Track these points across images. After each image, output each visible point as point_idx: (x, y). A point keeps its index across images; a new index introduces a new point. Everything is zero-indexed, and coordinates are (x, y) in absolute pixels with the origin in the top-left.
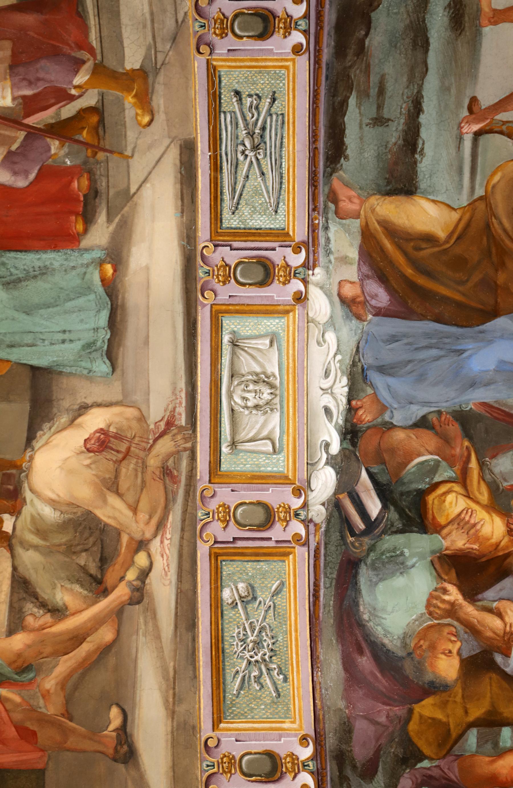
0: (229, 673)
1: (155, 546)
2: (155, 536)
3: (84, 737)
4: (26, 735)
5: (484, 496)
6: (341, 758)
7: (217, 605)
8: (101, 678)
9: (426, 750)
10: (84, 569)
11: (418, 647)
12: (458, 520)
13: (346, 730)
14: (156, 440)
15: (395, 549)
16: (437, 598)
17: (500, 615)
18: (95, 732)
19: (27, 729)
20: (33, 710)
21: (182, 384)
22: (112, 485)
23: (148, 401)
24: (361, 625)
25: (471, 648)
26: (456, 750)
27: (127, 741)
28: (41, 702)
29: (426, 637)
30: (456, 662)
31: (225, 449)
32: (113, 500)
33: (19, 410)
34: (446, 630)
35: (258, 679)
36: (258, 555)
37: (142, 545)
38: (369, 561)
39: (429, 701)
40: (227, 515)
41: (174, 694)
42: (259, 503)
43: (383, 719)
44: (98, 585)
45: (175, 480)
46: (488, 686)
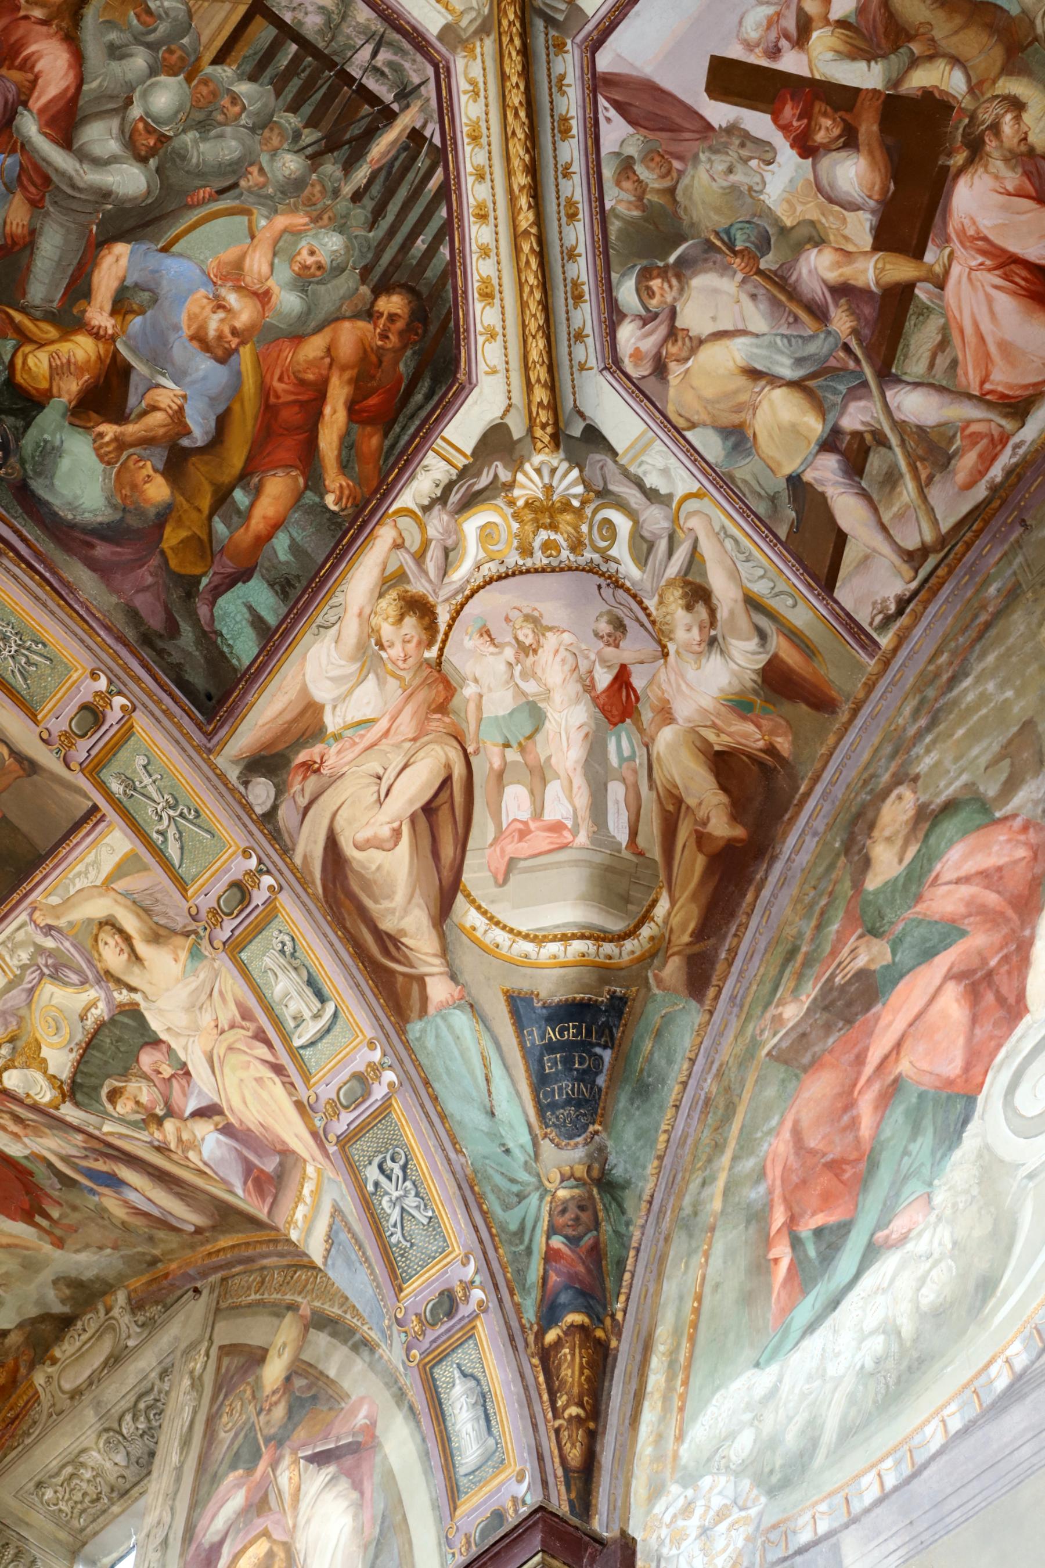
5: (52, 332)
6: (147, 639)
9: (197, 571)
11: (124, 498)
12: (55, 371)
13: (133, 615)
15: (38, 445)
16: (101, 447)
17: (155, 408)
24: (73, 526)
25: (159, 456)
26: (217, 548)
29: (123, 485)
30: (159, 480)
34: (131, 463)
35: (29, 662)
38: (30, 473)
39: (168, 530)
43: (150, 580)
46: (198, 471)
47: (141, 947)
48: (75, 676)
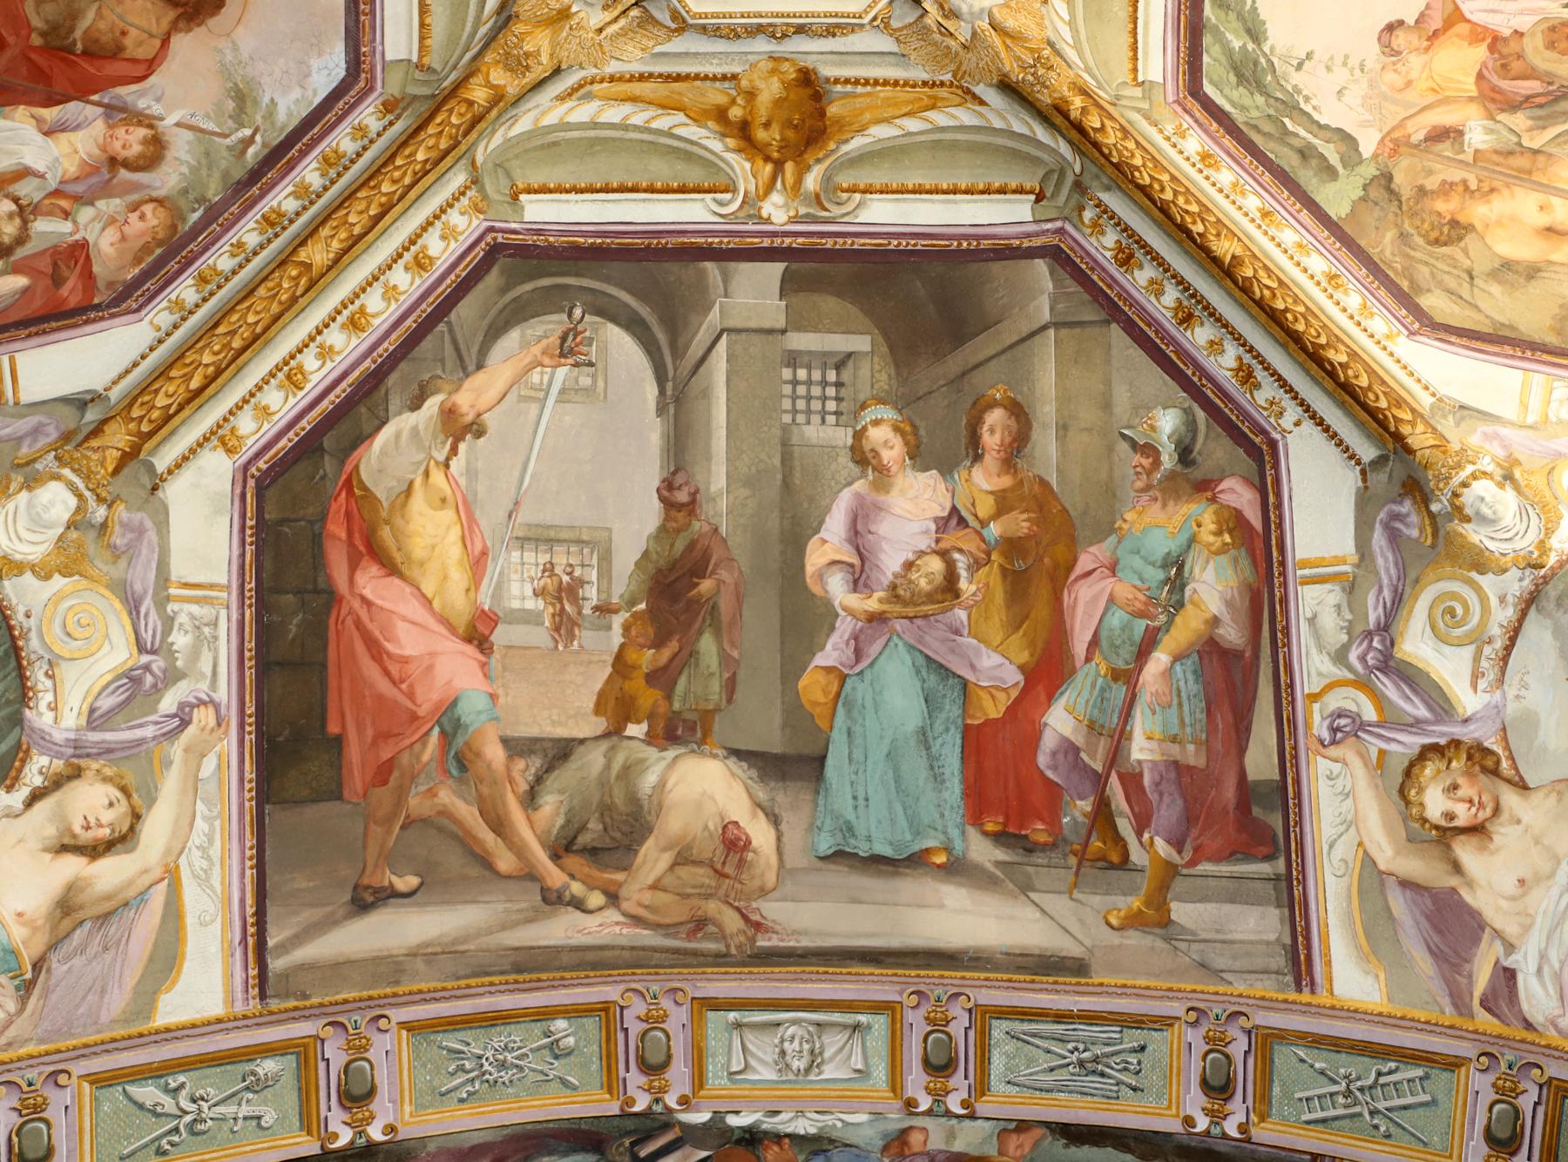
0: (467, 1035)
1: (613, 915)
2: (624, 914)
3: (382, 846)
4: (383, 773)
7: (545, 1014)
8: (453, 860)
10: (583, 828)
14: (738, 909)
18: (391, 860)
19: (390, 773)
20: (413, 778)
21: (805, 943)
22: (684, 858)
23: (785, 900)
27: (379, 900)
28: (422, 788)
31: (732, 1016)
32: (666, 859)
33: (773, 740)
36: (609, 1059)
37: (613, 898)
40: (654, 1020)
41: (436, 954)
42: (669, 1057)
44: (563, 847)
45: (691, 935)
47: (73, 865)
48: (407, 1108)
